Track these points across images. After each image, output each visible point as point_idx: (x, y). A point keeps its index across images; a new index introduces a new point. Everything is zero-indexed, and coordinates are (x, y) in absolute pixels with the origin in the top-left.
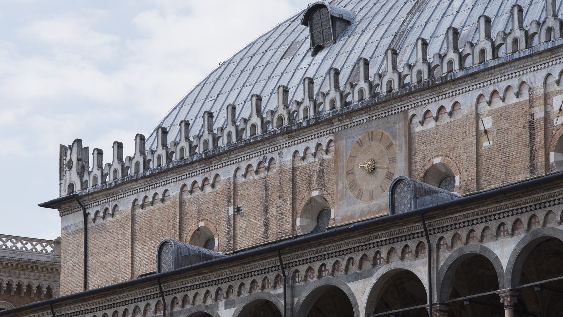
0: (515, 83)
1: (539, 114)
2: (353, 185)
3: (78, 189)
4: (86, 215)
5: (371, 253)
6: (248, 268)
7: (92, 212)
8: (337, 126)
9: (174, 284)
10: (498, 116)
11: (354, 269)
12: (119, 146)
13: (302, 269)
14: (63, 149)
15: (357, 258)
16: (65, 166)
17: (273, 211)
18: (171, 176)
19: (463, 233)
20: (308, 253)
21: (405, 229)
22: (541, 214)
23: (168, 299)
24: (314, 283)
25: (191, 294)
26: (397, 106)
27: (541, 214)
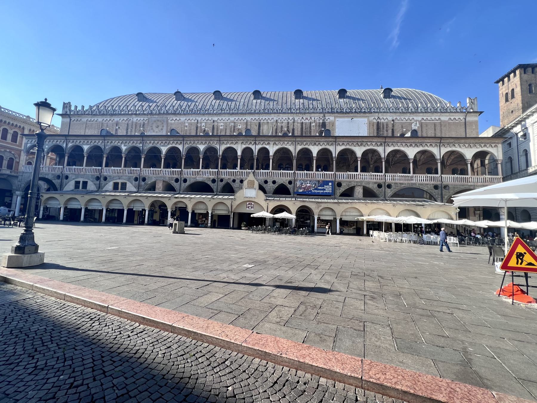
0: (194, 118)
1: (199, 125)
2: (152, 129)
3: (68, 113)
4: (70, 120)
5: (168, 142)
6: (132, 139)
7: (73, 119)
8: (149, 116)
9: (108, 138)
10: (190, 124)
11: (162, 144)
12: (83, 107)
13: (148, 142)
14: (64, 104)
15: (164, 142)
16: (64, 108)
17: (129, 130)
18: (100, 116)
19: (192, 142)
20: (151, 139)
21: (177, 139)
22: (211, 142)
23: (106, 141)
24: (151, 145)
25: (113, 141)
26: (165, 116)
27: (211, 142)
